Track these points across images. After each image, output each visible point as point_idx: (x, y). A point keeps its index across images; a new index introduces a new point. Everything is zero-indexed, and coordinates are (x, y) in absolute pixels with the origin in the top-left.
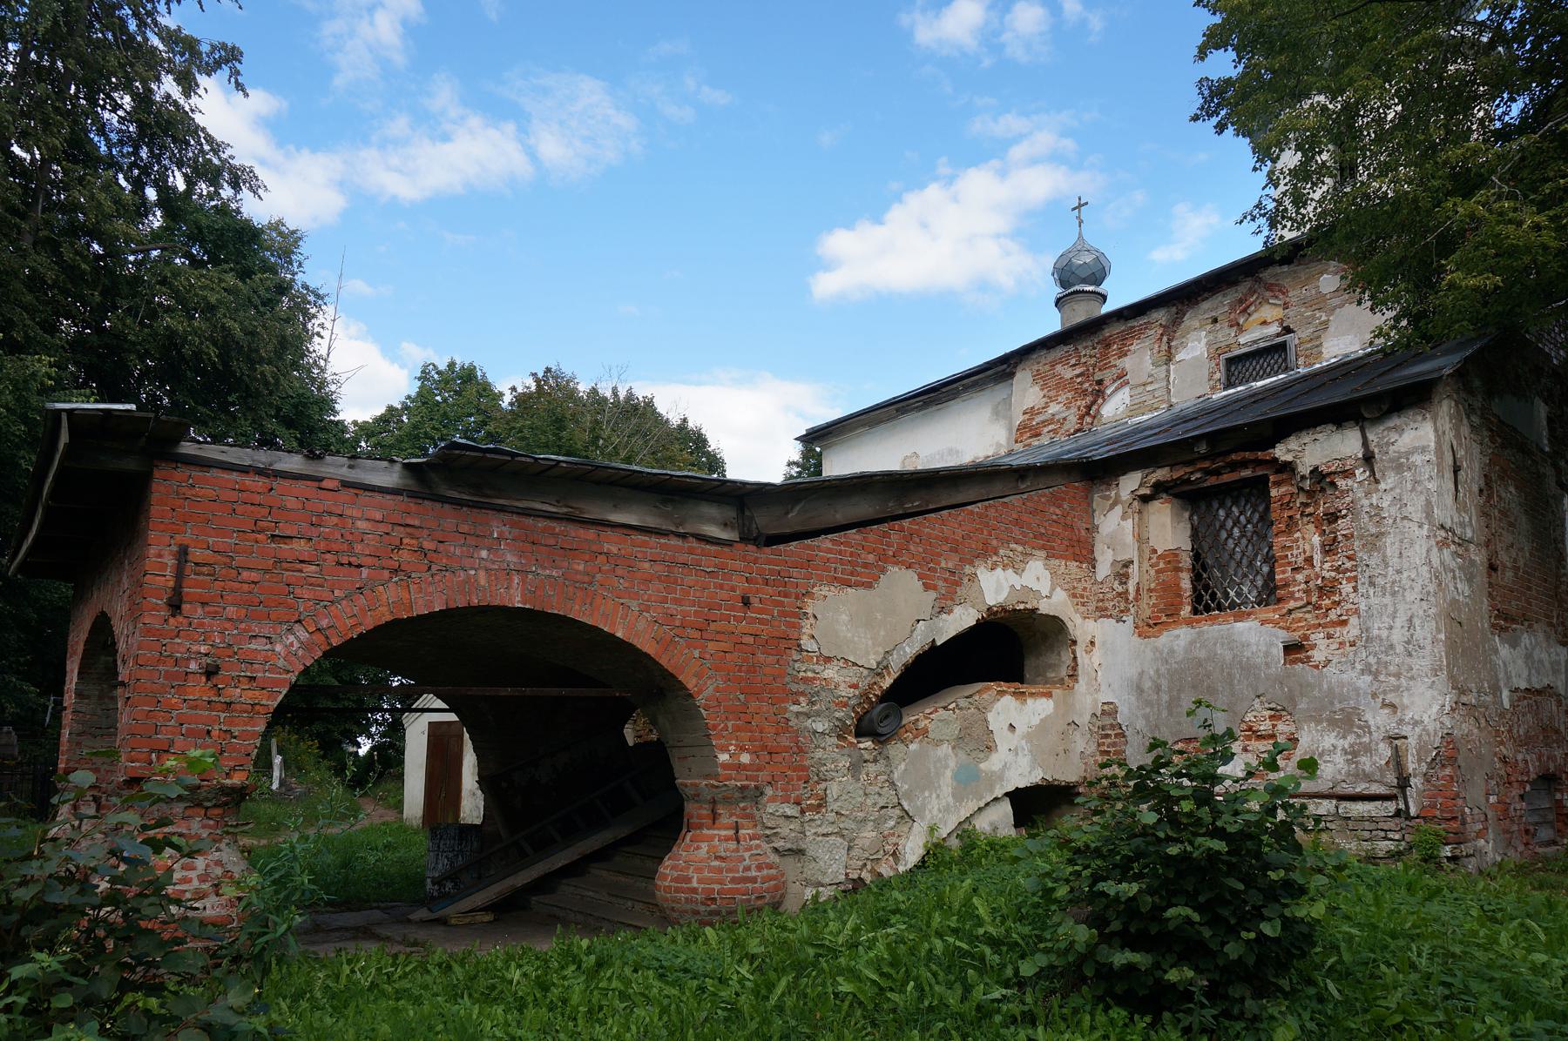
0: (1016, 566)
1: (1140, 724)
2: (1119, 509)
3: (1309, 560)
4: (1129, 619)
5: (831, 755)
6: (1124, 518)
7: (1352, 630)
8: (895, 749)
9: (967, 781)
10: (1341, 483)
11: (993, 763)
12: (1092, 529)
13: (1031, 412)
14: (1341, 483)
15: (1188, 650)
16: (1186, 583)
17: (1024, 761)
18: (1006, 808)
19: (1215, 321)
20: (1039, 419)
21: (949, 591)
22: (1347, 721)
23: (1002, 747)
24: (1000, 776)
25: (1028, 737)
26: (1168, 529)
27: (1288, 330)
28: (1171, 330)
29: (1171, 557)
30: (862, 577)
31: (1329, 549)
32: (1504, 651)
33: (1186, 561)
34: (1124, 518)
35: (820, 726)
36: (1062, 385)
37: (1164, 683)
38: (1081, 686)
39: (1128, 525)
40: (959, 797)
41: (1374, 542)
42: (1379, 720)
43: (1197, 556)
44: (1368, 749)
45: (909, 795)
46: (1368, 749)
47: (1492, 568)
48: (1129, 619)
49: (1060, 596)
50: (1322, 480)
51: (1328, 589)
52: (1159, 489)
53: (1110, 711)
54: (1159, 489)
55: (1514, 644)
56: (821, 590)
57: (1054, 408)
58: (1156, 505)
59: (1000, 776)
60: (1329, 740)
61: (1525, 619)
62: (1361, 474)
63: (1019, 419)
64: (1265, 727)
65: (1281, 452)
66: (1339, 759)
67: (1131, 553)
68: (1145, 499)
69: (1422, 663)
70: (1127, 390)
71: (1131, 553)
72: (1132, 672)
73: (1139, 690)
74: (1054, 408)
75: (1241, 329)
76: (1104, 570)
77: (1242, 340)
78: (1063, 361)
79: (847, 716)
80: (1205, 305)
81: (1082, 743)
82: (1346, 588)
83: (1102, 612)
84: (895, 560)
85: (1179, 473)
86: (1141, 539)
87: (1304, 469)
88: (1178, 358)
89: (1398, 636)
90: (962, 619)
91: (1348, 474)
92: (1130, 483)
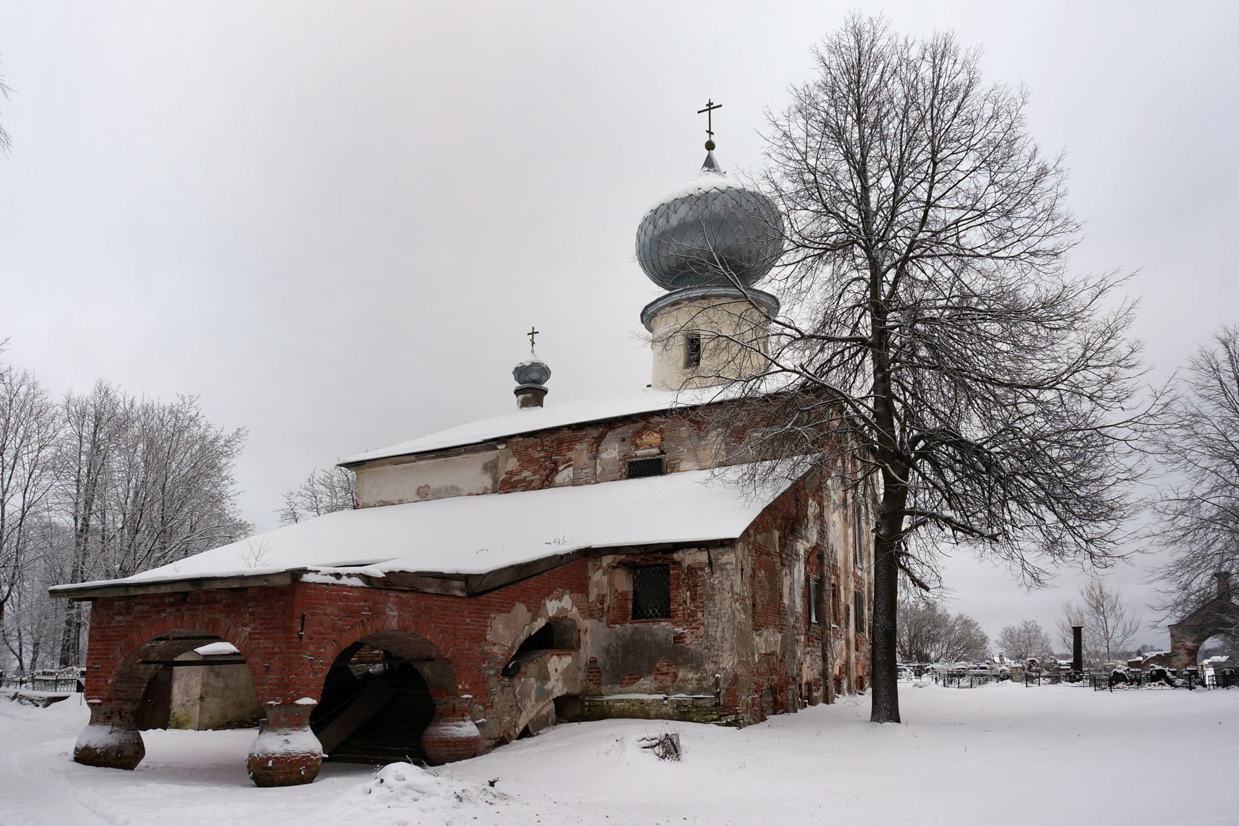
0: (560, 599)
1: (608, 667)
2: (601, 571)
3: (685, 602)
4: (604, 619)
5: (495, 685)
6: (604, 574)
7: (701, 632)
8: (516, 681)
9: (542, 694)
10: (700, 573)
11: (549, 686)
12: (588, 578)
13: (511, 473)
14: (700, 573)
15: (632, 634)
16: (630, 606)
17: (560, 684)
18: (552, 705)
19: (624, 440)
20: (515, 478)
21: (536, 610)
22: (698, 668)
23: (553, 679)
24: (551, 691)
25: (562, 674)
26: (624, 583)
27: (662, 452)
28: (599, 440)
29: (624, 594)
30: (506, 608)
31: (693, 599)
32: (757, 639)
33: (631, 597)
34: (604, 574)
35: (492, 672)
36: (532, 461)
37: (620, 650)
38: (582, 650)
39: (605, 578)
40: (537, 701)
41: (711, 598)
42: (709, 667)
43: (635, 594)
44: (705, 679)
45: (521, 701)
46: (705, 679)
47: (754, 605)
48: (604, 619)
49: (575, 609)
50: (692, 571)
51: (693, 614)
52: (620, 563)
53: (593, 661)
54: (621, 564)
55: (760, 635)
56: (492, 616)
57: (526, 474)
58: (618, 570)
59: (551, 691)
60: (690, 675)
61: (765, 625)
62: (707, 570)
63: (503, 476)
64: (665, 670)
65: (675, 556)
66: (694, 682)
67: (606, 591)
68: (614, 568)
69: (727, 646)
70: (571, 469)
71: (606, 591)
72: (605, 644)
73: (608, 652)
74: (526, 474)
75: (637, 447)
76: (592, 598)
77: (639, 453)
78: (534, 446)
79: (500, 667)
80: (618, 430)
81: (581, 676)
82: (700, 615)
83: (591, 616)
84: (517, 599)
85: (631, 559)
86: (611, 584)
87: (685, 565)
88: (604, 456)
89: (718, 635)
90: (541, 623)
91: (703, 569)
92: (607, 560)
